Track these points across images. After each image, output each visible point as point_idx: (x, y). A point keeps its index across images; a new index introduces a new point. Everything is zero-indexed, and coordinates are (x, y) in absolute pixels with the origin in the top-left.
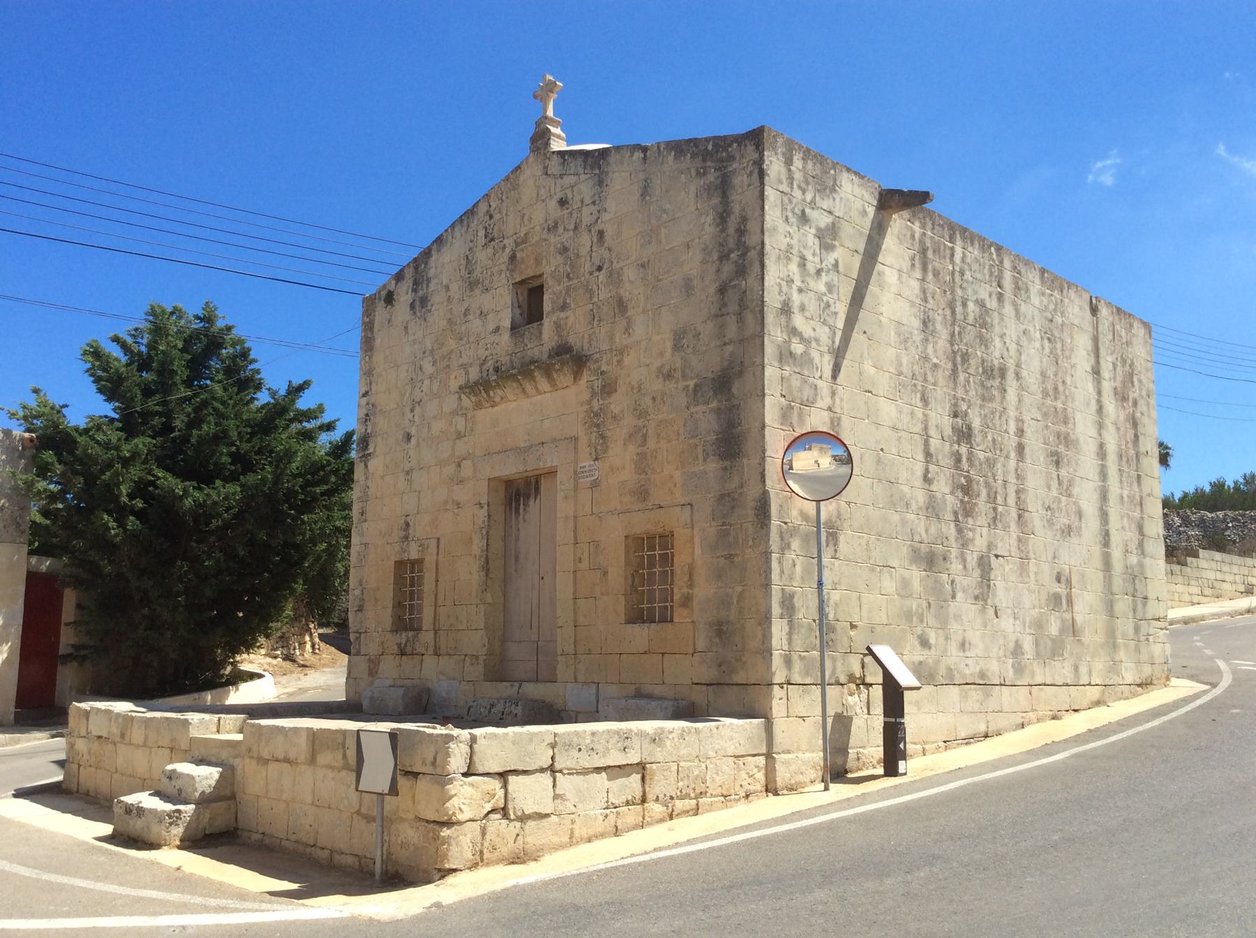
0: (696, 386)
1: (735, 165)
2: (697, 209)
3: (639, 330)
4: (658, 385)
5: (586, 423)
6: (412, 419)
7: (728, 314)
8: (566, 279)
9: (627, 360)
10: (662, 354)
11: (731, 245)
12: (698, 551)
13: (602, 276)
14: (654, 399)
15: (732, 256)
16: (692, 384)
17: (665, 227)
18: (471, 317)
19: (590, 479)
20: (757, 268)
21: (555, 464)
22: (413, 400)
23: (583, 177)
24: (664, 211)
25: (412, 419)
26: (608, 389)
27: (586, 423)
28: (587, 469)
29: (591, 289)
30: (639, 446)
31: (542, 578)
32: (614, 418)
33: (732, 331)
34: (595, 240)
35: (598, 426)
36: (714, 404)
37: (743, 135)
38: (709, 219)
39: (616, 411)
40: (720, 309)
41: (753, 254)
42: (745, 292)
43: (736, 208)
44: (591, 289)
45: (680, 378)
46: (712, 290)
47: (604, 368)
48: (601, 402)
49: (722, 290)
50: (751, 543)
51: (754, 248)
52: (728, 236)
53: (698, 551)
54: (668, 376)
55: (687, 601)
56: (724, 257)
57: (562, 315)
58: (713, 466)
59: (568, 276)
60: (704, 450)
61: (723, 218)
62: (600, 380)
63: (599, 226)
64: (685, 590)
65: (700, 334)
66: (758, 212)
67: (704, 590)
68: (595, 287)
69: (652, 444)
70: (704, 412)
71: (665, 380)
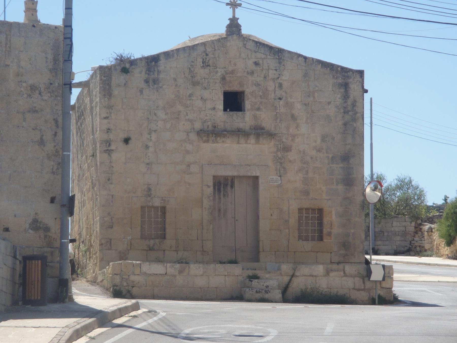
0: (333, 157)
1: (351, 80)
2: (333, 90)
3: (304, 129)
4: (314, 153)
5: (274, 161)
6: (149, 138)
7: (348, 134)
8: (259, 98)
9: (297, 140)
10: (315, 142)
11: (349, 108)
12: (334, 216)
13: (282, 102)
14: (312, 158)
15: (350, 113)
16: (330, 156)
17: (317, 93)
18: (194, 98)
19: (276, 183)
20: (361, 120)
21: (258, 175)
22: (150, 129)
23: (269, 57)
24: (317, 86)
25: (149, 138)
26: (287, 149)
27: (274, 161)
28: (274, 179)
29: (276, 107)
30: (304, 175)
31: (237, 220)
32: (290, 161)
33: (349, 140)
34: (277, 86)
35: (281, 163)
36: (341, 165)
37: (355, 70)
38: (339, 96)
39: (292, 159)
40: (344, 131)
41: (359, 115)
42: (355, 128)
43: (352, 96)
44: (276, 107)
45: (325, 152)
46: (340, 123)
47: (284, 140)
48: (282, 154)
49: (345, 124)
50: (358, 216)
51: (360, 113)
52: (348, 105)
53: (334, 216)
54: (319, 151)
55: (329, 234)
56: (346, 112)
57: (257, 113)
58: (341, 187)
59: (261, 96)
60: (336, 181)
61: (346, 97)
62: (282, 145)
63: (279, 81)
64: (329, 230)
65: (334, 138)
66: (361, 101)
67: (336, 230)
68: (278, 106)
69: (311, 175)
70: (336, 167)
71: (317, 152)
